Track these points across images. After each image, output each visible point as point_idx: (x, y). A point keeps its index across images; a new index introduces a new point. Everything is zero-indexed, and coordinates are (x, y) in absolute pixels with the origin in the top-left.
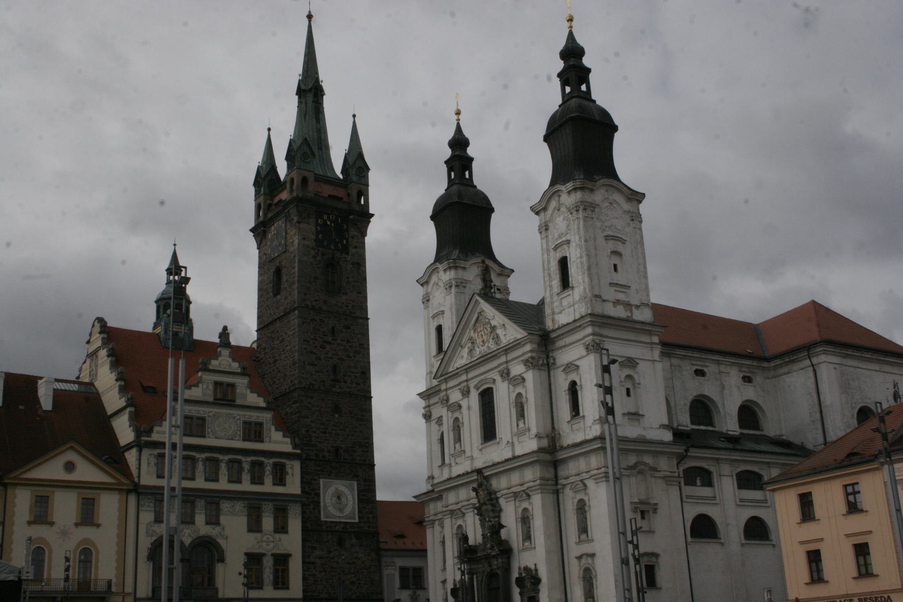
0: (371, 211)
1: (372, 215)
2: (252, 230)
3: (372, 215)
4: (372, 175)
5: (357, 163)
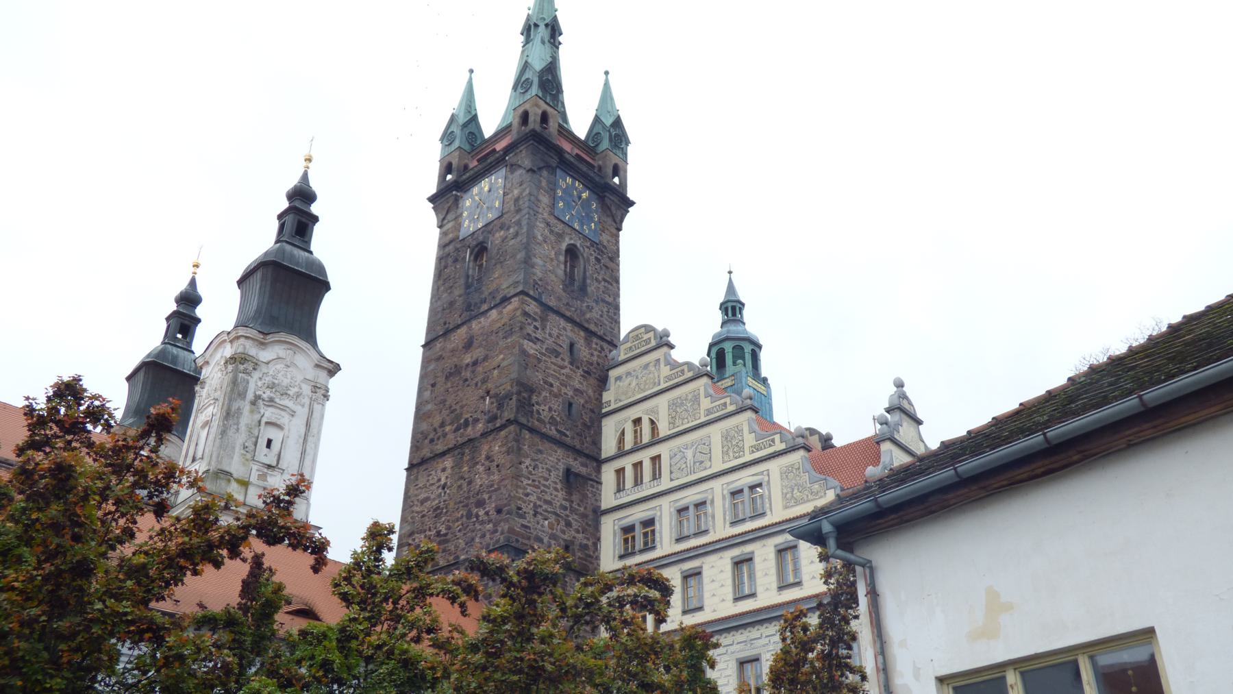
0: (631, 195)
1: (632, 203)
2: (432, 199)
3: (632, 203)
4: (631, 150)
5: (612, 133)
